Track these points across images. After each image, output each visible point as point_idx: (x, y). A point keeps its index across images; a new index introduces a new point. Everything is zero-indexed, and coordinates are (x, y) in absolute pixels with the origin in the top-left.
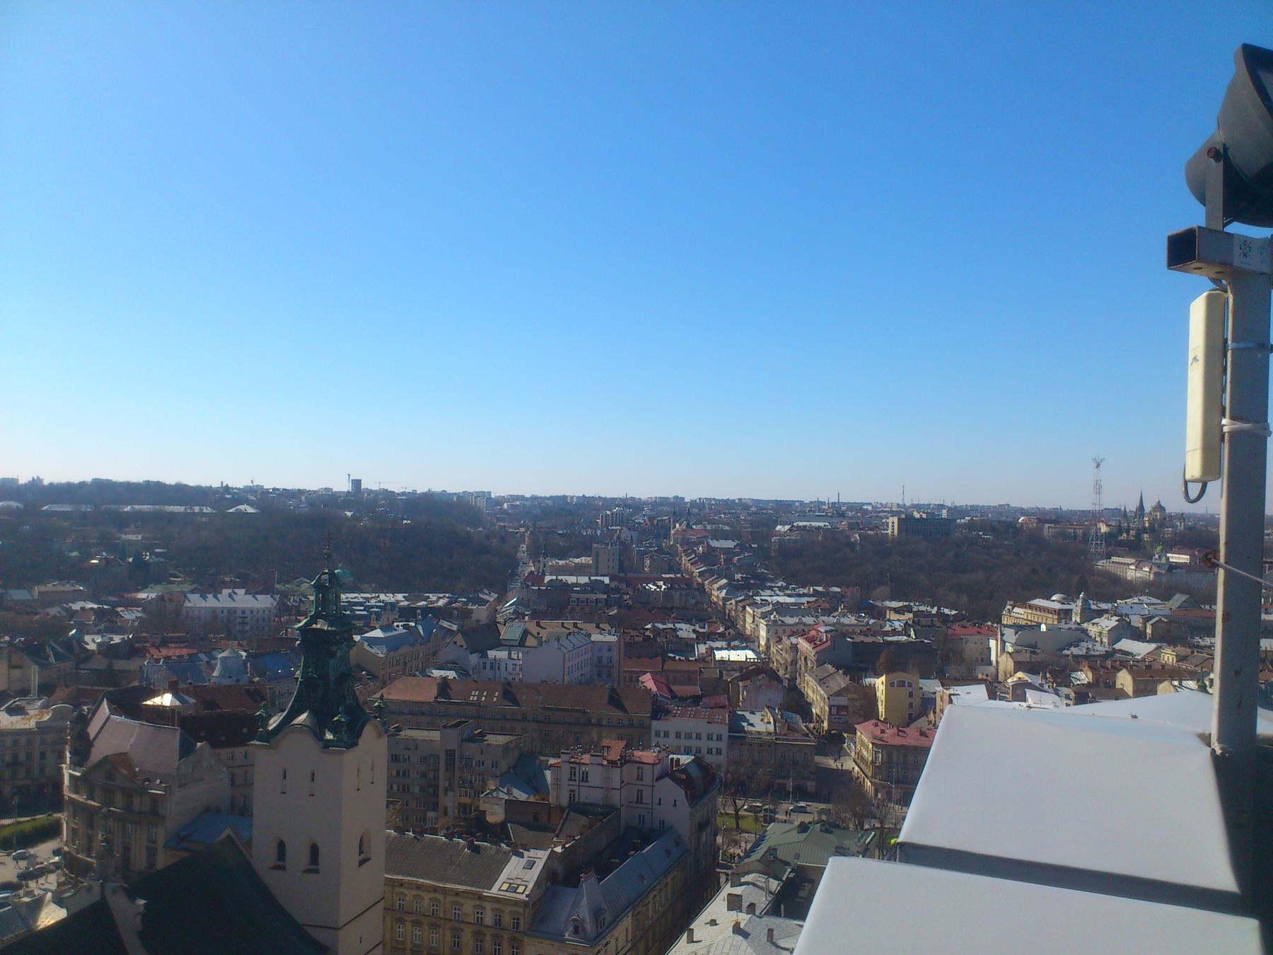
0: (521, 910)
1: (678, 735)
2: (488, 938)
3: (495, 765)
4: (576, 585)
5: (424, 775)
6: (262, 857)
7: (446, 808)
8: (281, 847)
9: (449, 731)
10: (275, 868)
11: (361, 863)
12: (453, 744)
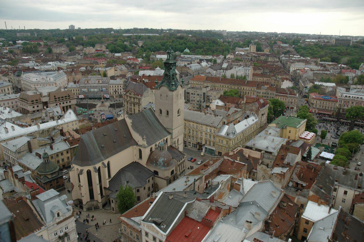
0: (216, 129)
1: (263, 93)
2: (208, 135)
6: (157, 114)
7: (203, 106)
9: (204, 88)
11: (178, 116)
12: (205, 92)
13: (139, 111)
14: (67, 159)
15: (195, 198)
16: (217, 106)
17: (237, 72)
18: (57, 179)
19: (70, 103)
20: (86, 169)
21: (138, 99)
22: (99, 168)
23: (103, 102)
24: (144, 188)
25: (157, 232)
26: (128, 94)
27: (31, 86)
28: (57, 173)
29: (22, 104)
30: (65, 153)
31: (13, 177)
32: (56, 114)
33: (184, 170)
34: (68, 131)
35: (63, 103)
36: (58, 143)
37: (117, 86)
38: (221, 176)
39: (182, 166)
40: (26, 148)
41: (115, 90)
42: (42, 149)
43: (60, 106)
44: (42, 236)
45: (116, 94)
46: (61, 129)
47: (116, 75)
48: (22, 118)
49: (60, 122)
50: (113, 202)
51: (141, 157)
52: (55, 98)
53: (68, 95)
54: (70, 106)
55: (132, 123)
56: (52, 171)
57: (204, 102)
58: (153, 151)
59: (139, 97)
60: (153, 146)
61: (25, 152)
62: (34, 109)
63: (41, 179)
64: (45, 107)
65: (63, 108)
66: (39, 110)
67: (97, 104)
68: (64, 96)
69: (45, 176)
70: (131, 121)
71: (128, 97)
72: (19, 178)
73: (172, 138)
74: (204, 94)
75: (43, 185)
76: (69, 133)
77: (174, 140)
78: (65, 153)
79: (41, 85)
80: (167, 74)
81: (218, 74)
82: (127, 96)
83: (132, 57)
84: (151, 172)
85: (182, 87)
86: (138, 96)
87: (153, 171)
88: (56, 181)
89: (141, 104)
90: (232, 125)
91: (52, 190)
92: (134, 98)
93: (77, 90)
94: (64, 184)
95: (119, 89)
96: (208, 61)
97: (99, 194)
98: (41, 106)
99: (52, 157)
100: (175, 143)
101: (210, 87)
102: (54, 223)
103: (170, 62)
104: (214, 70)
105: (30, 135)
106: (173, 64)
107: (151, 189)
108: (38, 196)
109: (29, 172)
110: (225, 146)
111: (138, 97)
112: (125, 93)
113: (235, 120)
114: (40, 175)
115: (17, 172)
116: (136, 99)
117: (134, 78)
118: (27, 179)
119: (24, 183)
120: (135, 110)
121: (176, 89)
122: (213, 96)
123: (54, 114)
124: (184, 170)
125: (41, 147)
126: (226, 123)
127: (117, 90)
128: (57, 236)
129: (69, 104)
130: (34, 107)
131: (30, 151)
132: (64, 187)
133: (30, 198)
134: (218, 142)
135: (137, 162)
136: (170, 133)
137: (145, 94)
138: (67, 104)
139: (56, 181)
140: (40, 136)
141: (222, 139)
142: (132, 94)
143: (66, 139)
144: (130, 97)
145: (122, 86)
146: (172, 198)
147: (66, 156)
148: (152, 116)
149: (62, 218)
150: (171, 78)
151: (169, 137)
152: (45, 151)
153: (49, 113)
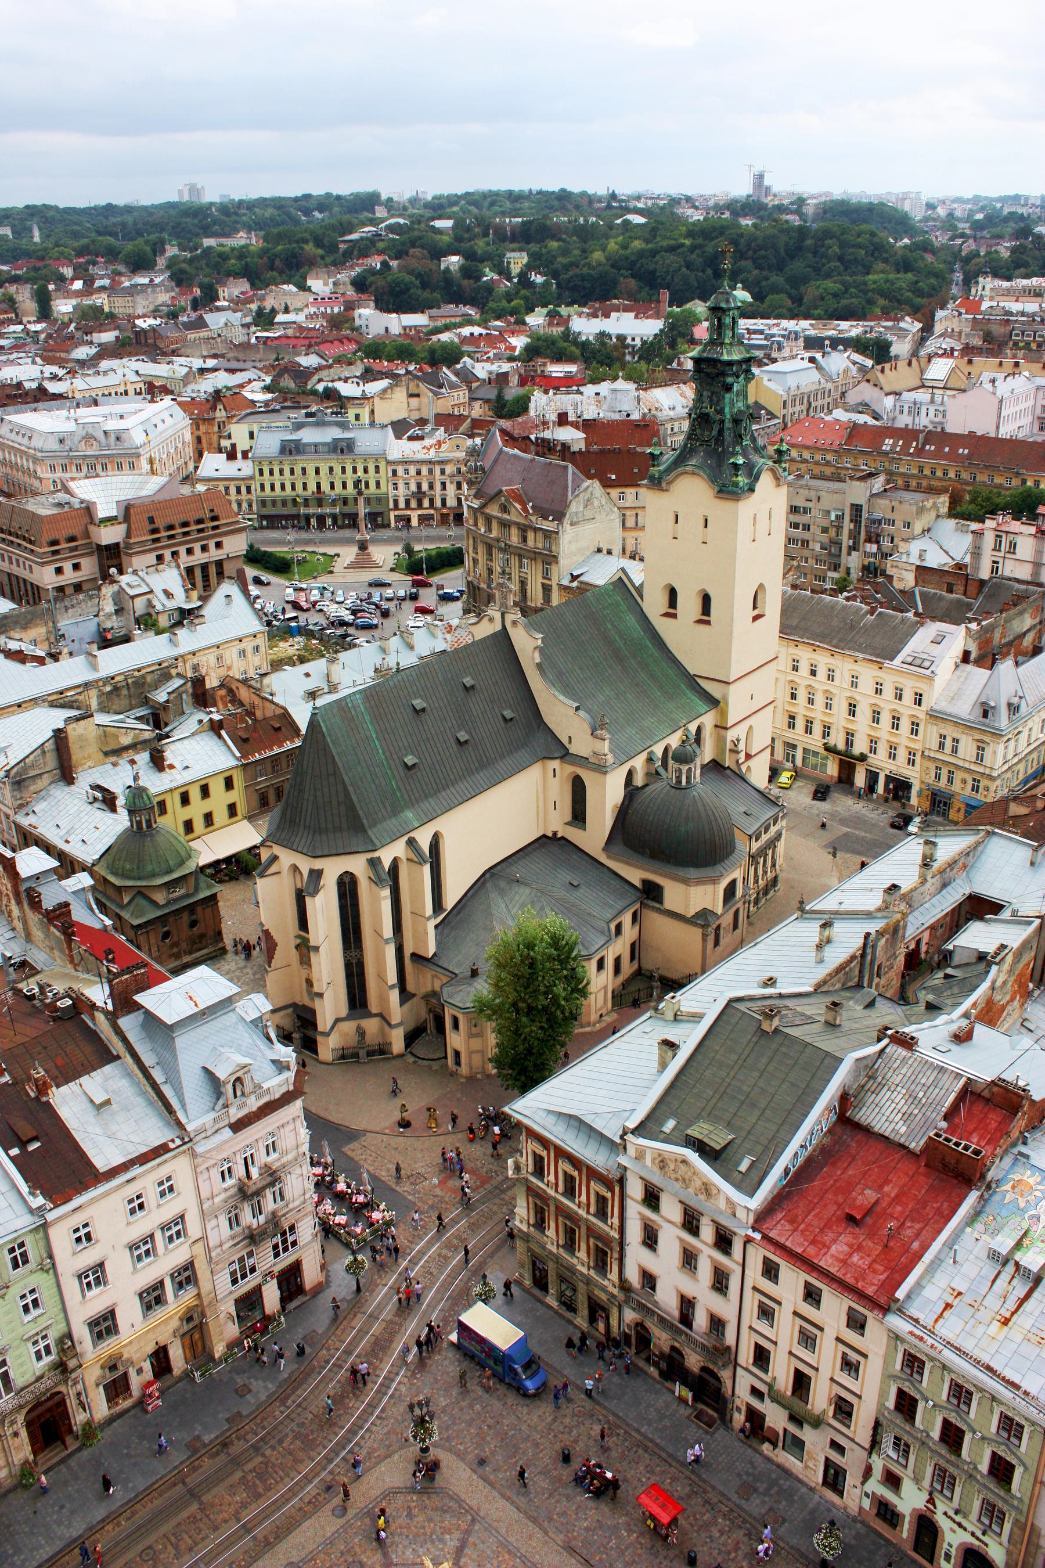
3: (908, 525)
4: (1023, 314)
5: (825, 530)
6: (654, 605)
7: (848, 570)
8: (673, 593)
9: (858, 483)
10: (667, 615)
11: (755, 618)
12: (862, 500)
13: (547, 589)
14: (225, 812)
15: (889, 1032)
16: (918, 567)
17: (1001, 401)
18: (191, 908)
19: (220, 552)
20: (333, 869)
21: (540, 535)
22: (395, 863)
23: (363, 546)
24: (601, 965)
25: (707, 1189)
26: (493, 510)
27: (39, 470)
28: (192, 881)
29: (10, 558)
30: (217, 787)
31: (19, 903)
32: (160, 602)
33: (775, 881)
34: (222, 686)
35: (190, 551)
36: (185, 741)
37: (424, 471)
38: (987, 921)
39: (769, 858)
40: (51, 762)
41: (419, 485)
42: (115, 765)
43: (178, 567)
44: (169, 1179)
45: (420, 505)
46: (190, 674)
47: (416, 416)
48: (16, 623)
49: (187, 639)
50: (456, 1026)
51: (579, 816)
52: (153, 526)
53: (208, 515)
54: (219, 564)
55: (540, 650)
56: (170, 871)
57: (854, 548)
58: (638, 788)
59: (548, 525)
60: (639, 763)
61: (46, 779)
62: (61, 578)
63: (122, 907)
64: (113, 571)
65: (190, 571)
66: (85, 587)
67: (338, 555)
68: (191, 517)
69: (141, 893)
70: (539, 642)
71: (495, 524)
72: (45, 905)
73: (721, 727)
74: (857, 509)
75: (132, 933)
76: (231, 691)
77: (731, 735)
78: (217, 787)
79: (79, 468)
80: (707, 415)
81: (906, 410)
82: (488, 520)
83: (484, 332)
84: (627, 887)
85: (777, 479)
86: (546, 519)
87: (637, 883)
88: (186, 918)
89: (555, 557)
90: (1006, 666)
91: (203, 971)
92: (523, 530)
93: (244, 490)
94: (220, 933)
95: (438, 486)
96: (859, 345)
97: (390, 983)
98: (89, 566)
99: (162, 806)
100: (735, 751)
101: (882, 478)
102: (222, 1124)
103: (725, 357)
104: (887, 394)
105: (59, 700)
106: (739, 363)
107: (628, 968)
108: (140, 998)
109: (83, 880)
110: (967, 765)
111: (545, 522)
112: (476, 503)
113: (1015, 639)
114: (119, 889)
115: (37, 877)
116: (530, 535)
117: (516, 435)
118: (80, 914)
119: (73, 934)
120: (529, 587)
121: (752, 490)
122: (899, 524)
123: (155, 602)
124: (775, 881)
125: (113, 759)
126: (973, 657)
127: (425, 487)
128: (230, 1182)
129: (214, 554)
130: (59, 571)
131: (66, 775)
132: (221, 945)
133: (110, 1007)
134: (935, 745)
135: (563, 838)
136: (713, 702)
137: (575, 507)
138: (206, 555)
139: (186, 918)
140: (104, 709)
141: (956, 736)
142: (513, 510)
143: (221, 721)
144: (505, 525)
145: (449, 469)
146: (776, 1031)
147: (219, 799)
148: (631, 620)
149: (253, 1104)
150: (727, 433)
151: (708, 720)
152: (136, 778)
153: (133, 597)
